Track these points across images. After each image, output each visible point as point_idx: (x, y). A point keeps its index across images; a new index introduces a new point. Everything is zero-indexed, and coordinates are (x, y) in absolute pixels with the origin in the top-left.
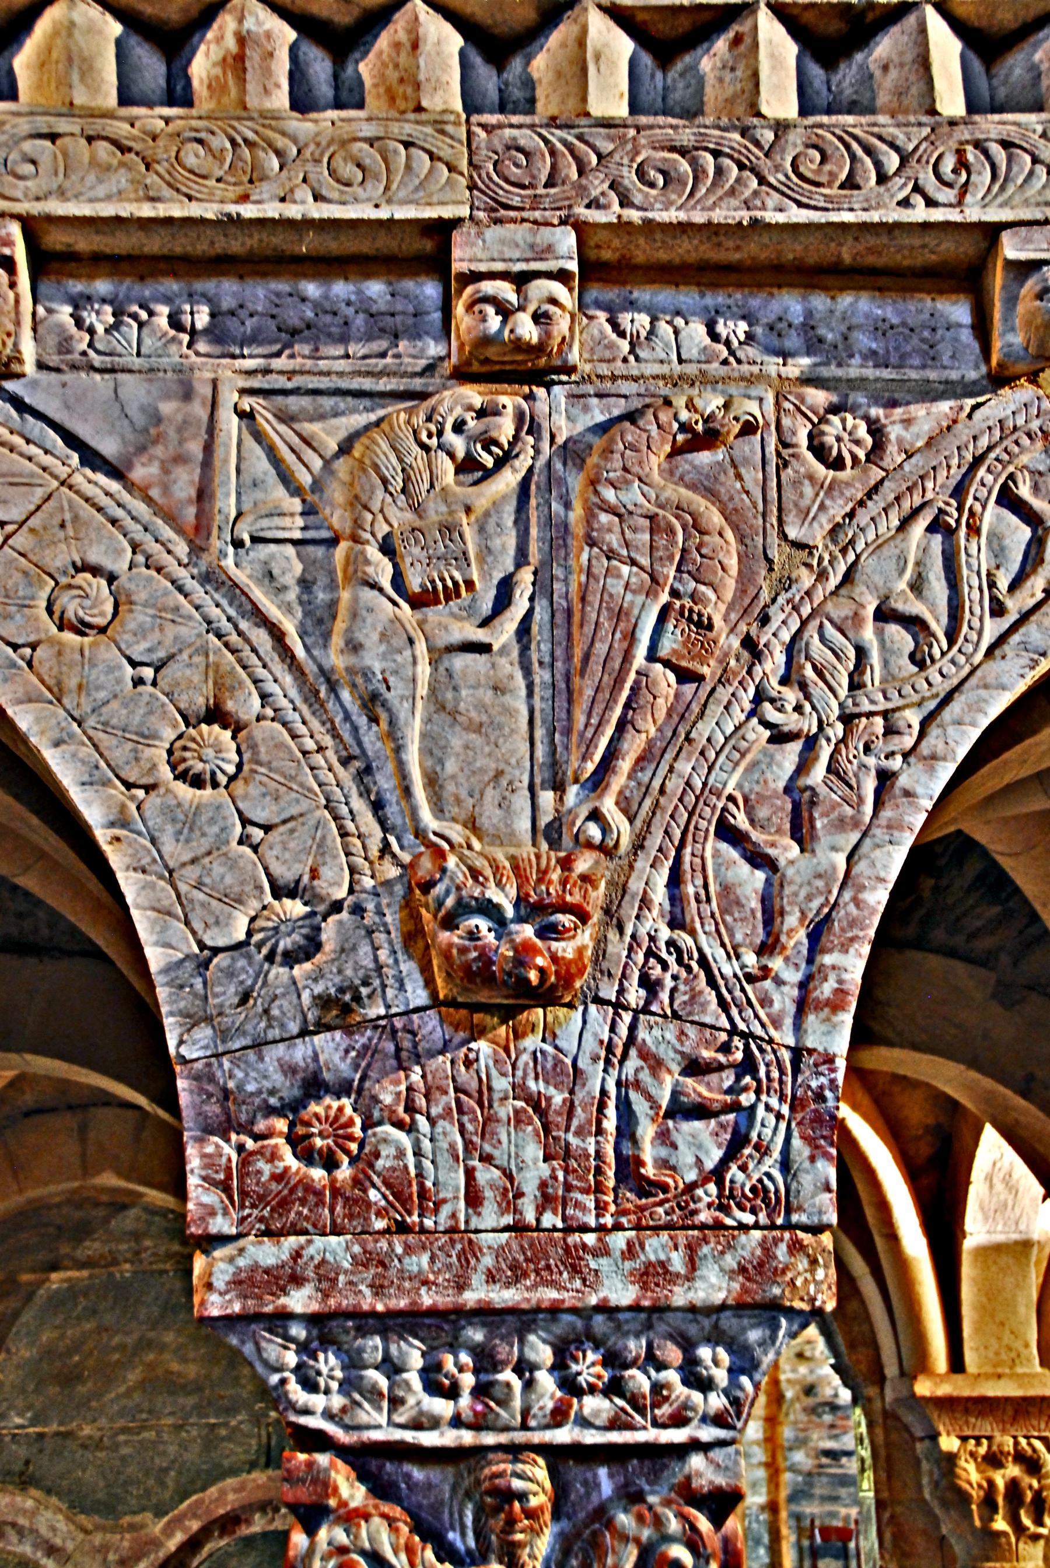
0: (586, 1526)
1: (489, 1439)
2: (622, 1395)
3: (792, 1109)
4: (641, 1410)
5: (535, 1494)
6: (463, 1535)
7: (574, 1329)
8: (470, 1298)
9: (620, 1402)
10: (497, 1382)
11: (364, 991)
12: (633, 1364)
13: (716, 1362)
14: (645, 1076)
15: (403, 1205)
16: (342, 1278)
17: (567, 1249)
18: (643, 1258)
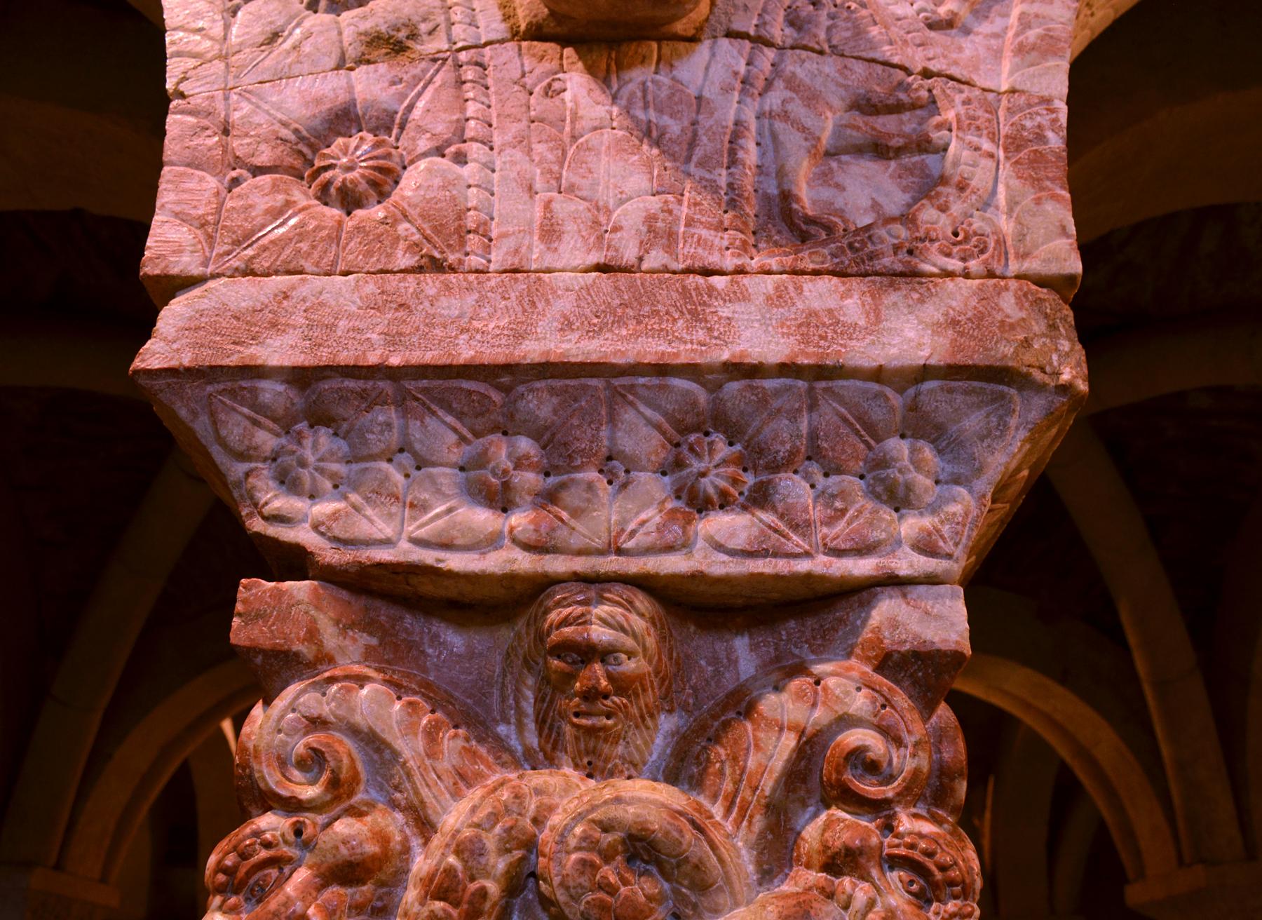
0: (715, 717)
1: (558, 565)
2: (774, 509)
3: (1006, 150)
4: (801, 527)
5: (631, 654)
6: (520, 727)
7: (694, 404)
8: (532, 350)
9: (768, 517)
10: (573, 480)
11: (424, 27)
12: (788, 463)
13: (918, 465)
14: (798, 109)
15: (445, 240)
16: (342, 324)
17: (685, 292)
18: (800, 305)
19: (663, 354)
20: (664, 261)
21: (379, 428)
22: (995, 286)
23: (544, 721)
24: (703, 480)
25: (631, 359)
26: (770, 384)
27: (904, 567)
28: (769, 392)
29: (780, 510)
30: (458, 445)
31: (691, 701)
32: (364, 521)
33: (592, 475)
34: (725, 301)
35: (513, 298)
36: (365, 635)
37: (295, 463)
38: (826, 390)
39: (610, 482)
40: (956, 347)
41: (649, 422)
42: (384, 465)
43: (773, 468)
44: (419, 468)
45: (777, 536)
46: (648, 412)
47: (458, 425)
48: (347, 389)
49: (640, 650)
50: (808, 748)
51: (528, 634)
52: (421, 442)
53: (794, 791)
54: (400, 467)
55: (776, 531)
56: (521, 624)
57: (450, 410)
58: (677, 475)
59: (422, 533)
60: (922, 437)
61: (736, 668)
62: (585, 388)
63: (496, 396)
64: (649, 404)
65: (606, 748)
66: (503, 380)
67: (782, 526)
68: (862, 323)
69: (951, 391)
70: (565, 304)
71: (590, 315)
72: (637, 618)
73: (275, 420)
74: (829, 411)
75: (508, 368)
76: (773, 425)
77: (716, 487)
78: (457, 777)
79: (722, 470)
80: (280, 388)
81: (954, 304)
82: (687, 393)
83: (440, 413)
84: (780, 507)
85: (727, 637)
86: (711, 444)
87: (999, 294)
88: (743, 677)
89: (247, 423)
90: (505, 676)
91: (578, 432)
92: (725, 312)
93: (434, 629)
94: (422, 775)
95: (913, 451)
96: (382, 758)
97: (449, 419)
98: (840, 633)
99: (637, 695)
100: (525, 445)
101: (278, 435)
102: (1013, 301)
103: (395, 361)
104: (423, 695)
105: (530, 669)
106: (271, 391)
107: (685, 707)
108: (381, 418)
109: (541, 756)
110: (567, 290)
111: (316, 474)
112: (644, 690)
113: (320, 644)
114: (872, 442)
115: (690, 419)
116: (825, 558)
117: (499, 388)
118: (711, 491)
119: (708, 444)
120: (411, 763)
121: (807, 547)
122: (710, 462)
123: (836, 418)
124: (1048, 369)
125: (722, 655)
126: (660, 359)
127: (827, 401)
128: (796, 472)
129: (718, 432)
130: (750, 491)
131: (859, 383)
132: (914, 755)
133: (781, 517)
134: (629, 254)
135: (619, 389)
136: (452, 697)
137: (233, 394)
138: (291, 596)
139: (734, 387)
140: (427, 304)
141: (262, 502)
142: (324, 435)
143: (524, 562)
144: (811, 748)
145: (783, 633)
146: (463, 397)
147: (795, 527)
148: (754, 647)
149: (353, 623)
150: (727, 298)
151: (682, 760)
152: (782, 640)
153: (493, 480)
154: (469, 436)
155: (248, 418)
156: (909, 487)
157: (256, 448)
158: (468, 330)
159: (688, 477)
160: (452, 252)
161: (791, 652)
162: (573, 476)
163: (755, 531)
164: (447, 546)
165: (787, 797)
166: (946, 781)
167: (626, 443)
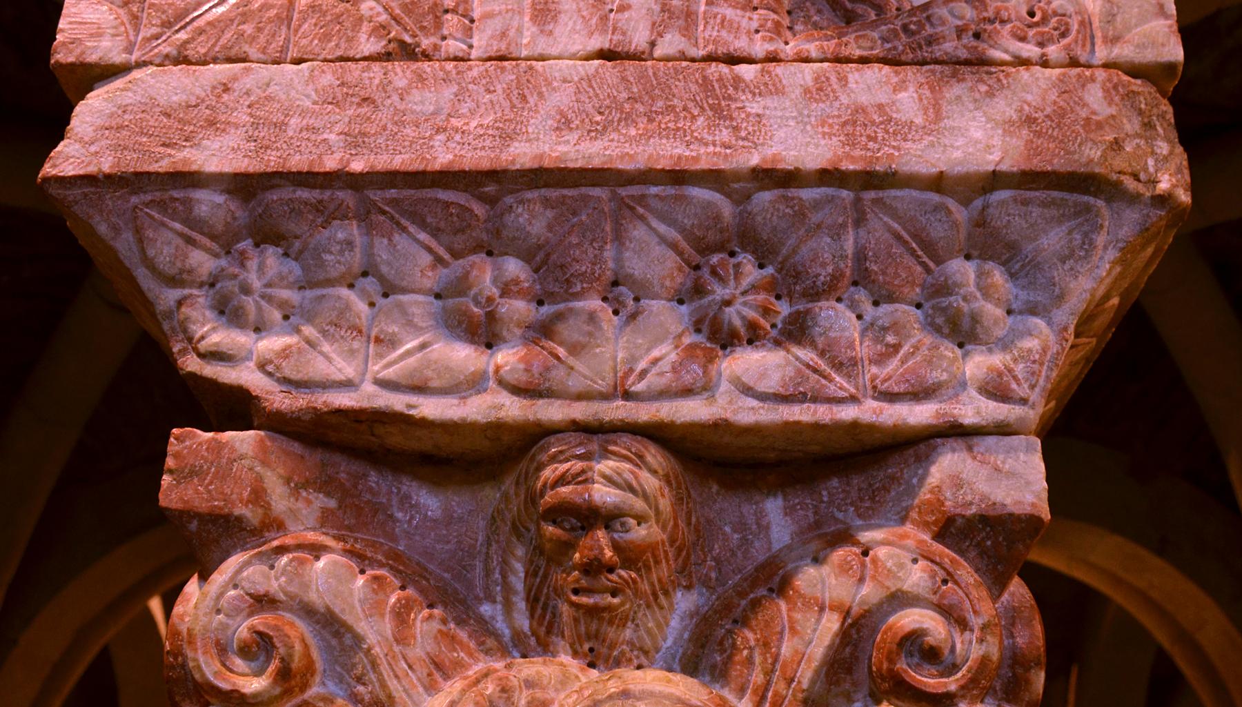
0: (742, 595)
1: (553, 412)
2: (813, 345)
4: (846, 366)
5: (641, 519)
6: (508, 606)
7: (718, 218)
9: (806, 354)
10: (571, 310)
12: (830, 290)
13: (986, 291)
16: (294, 122)
17: (706, 84)
18: (844, 99)
19: (679, 158)
20: (680, 47)
21: (338, 247)
22: (1079, 76)
23: (536, 599)
24: (727, 310)
25: (640, 163)
26: (808, 194)
27: (970, 414)
28: (807, 204)
29: (820, 346)
30: (433, 267)
31: (713, 575)
32: (321, 358)
33: (594, 303)
34: (754, 94)
35: (500, 91)
36: (321, 496)
37: (236, 290)
38: (876, 201)
39: (616, 312)
40: (1032, 150)
41: (663, 240)
42: (344, 292)
43: (811, 295)
44: (386, 295)
45: (817, 376)
46: (662, 228)
47: (433, 244)
48: (300, 201)
49: (652, 513)
50: (853, 631)
51: (517, 495)
52: (389, 264)
53: (837, 683)
54: (364, 294)
55: (815, 371)
56: (508, 483)
57: (423, 225)
58: (696, 304)
59: (389, 373)
60: (991, 258)
61: (768, 536)
62: (585, 199)
63: (479, 209)
64: (663, 218)
65: (611, 632)
66: (486, 189)
67: (822, 365)
68: (919, 120)
69: (1025, 203)
70: (561, 98)
71: (592, 111)
72: (648, 475)
73: (213, 238)
74: (879, 228)
75: (494, 175)
76: (812, 244)
77: (743, 318)
78: (432, 667)
79: (751, 297)
80: (220, 199)
81: (1029, 98)
82: (709, 205)
83: (412, 229)
84: (821, 342)
85: (757, 498)
86: (737, 266)
87: (1083, 86)
88: (776, 546)
89: (180, 241)
90: (489, 545)
91: (578, 252)
92: (754, 107)
93: (405, 488)
94: (390, 664)
95: (980, 274)
96: (341, 643)
97: (423, 236)
98: (893, 493)
99: (648, 568)
100: (513, 267)
101: (216, 256)
102: (1100, 94)
103: (357, 166)
104: (391, 568)
105: (519, 536)
106: (208, 202)
107: (706, 583)
108: (340, 236)
109: (533, 641)
110: (565, 81)
111: (263, 303)
112: (657, 562)
113: (267, 507)
114: (931, 264)
115: (712, 237)
116: (875, 404)
117: (482, 198)
118: (737, 322)
119: (734, 266)
120: (377, 650)
121: (853, 390)
122: (736, 288)
123: (887, 235)
124: (1142, 176)
125: (751, 520)
126: (676, 164)
127: (876, 214)
128: (839, 300)
129: (746, 251)
130: (784, 322)
131: (915, 193)
132: (981, 641)
133: (822, 354)
134: (639, 38)
135: (627, 201)
136: (426, 570)
137: (162, 205)
138: (233, 450)
139: (765, 197)
140: (395, 98)
141: (197, 336)
142: (272, 256)
143: (513, 409)
144: (858, 631)
145: (825, 493)
146: (439, 210)
147: (838, 366)
148: (789, 511)
149: (307, 481)
150: (757, 91)
151: (703, 646)
152: (823, 502)
153: (476, 310)
154: (447, 257)
155: (181, 235)
156: (975, 318)
157: (190, 272)
158: (445, 130)
159: (709, 305)
160: (426, 36)
161: (833, 517)
162: (571, 304)
163: (790, 371)
164: (420, 389)
165: (829, 691)
166: (1020, 671)
167: (635, 266)
